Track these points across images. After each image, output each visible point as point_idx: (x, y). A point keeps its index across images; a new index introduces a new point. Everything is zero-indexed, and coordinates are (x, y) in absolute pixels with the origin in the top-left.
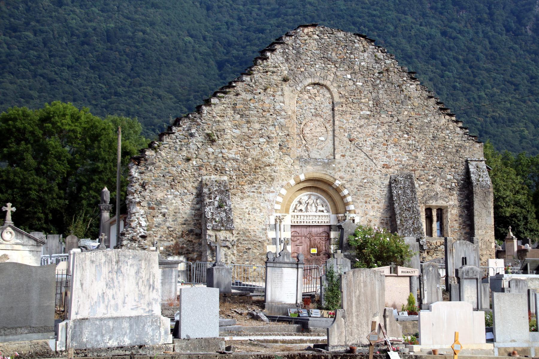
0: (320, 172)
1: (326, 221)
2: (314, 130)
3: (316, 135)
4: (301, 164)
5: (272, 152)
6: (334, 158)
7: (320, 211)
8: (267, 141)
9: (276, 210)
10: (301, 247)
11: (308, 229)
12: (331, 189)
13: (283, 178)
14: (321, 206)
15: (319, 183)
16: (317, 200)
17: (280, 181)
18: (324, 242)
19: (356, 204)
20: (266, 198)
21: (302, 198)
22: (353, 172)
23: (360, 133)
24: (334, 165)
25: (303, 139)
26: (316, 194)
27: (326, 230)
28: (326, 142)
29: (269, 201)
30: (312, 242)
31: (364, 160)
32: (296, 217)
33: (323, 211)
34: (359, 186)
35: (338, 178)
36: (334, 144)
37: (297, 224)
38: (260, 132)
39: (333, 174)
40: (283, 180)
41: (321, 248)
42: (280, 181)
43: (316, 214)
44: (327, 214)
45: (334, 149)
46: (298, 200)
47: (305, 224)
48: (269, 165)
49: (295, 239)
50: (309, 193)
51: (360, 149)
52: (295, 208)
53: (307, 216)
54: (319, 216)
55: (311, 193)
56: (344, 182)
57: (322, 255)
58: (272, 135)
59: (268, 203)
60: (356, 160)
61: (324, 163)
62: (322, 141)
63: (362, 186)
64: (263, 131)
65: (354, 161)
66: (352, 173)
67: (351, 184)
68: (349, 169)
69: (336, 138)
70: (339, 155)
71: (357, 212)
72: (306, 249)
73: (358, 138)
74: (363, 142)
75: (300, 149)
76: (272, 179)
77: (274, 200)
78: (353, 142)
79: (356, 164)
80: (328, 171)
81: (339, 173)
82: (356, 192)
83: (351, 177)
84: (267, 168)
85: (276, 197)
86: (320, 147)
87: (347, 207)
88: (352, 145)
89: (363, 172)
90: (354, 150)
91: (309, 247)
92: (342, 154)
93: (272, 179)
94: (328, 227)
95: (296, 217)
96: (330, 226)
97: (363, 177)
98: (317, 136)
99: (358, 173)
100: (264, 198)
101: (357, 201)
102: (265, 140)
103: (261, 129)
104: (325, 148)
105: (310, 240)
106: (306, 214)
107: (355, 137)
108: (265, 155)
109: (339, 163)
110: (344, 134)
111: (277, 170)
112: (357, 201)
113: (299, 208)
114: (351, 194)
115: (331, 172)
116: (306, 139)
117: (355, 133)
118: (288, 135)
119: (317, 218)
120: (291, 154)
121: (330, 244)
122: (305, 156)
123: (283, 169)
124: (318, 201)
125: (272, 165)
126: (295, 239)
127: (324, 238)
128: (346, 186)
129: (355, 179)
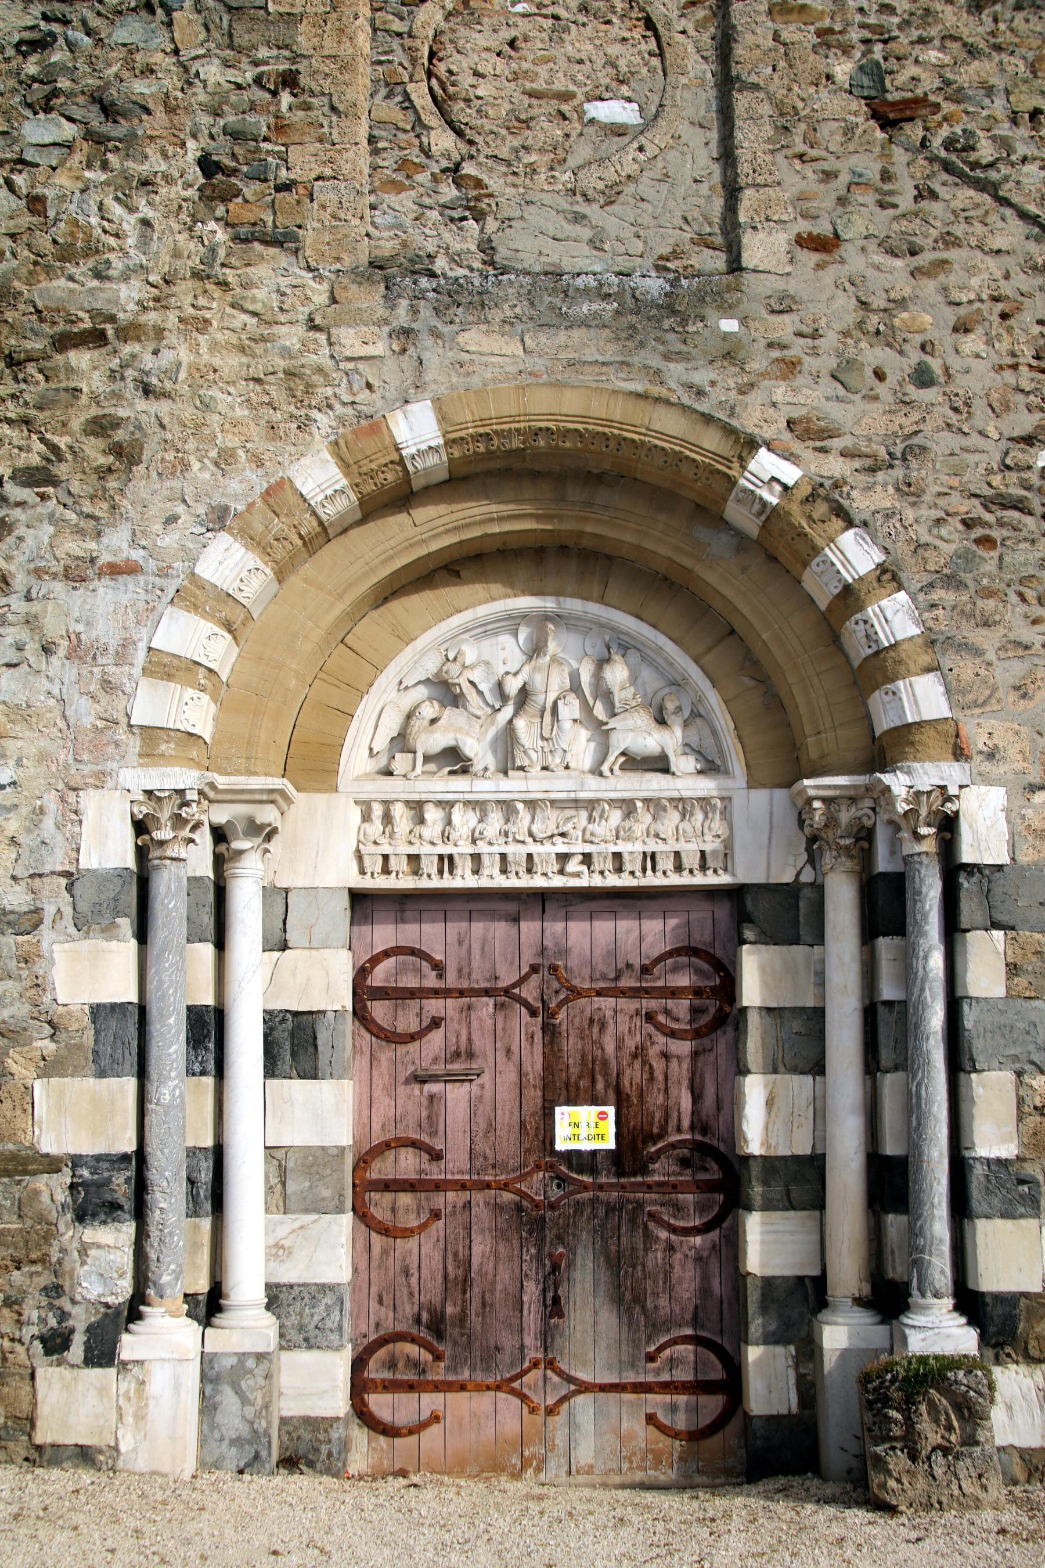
0: (588, 376)
1: (690, 851)
2: (536, 47)
3: (560, 84)
4: (402, 315)
5: (129, 224)
6: (735, 266)
7: (634, 763)
8: (89, 135)
9: (150, 734)
10: (457, 1095)
11: (530, 928)
12: (720, 544)
13: (232, 441)
14: (642, 719)
15: (603, 496)
16: (602, 663)
17: (201, 473)
18: (683, 1047)
19: (966, 668)
20: (53, 627)
21: (470, 654)
22: (923, 378)
23: (972, 51)
24: (729, 325)
25: (431, 118)
26: (595, 609)
27: (701, 937)
28: (657, 139)
29: (78, 651)
30: (571, 1046)
31: (1022, 281)
32: (399, 811)
33: (660, 764)
34: (988, 503)
35: (775, 430)
36: (727, 156)
37: (407, 883)
38: (31, 68)
39: (717, 395)
40: (225, 460)
41: (655, 1100)
42: (201, 473)
43: (593, 788)
44: (706, 786)
45: (732, 191)
46: (430, 666)
47: (492, 878)
48: (96, 338)
49: (408, 1020)
50: (526, 602)
51: (981, 185)
52: (402, 742)
53: (508, 807)
54: (628, 807)
55: (548, 604)
56: (835, 467)
57: (662, 1171)
58: (140, 87)
59: (71, 672)
60: (952, 280)
61: (639, 304)
62: (618, 131)
63: (1019, 506)
64: (58, 56)
65: (929, 287)
66: (914, 392)
67: (908, 490)
68: (874, 355)
69: (742, 102)
70: (782, 239)
71: (977, 738)
72: (507, 1115)
73: (958, 97)
74: (1004, 129)
75: (405, 202)
76: (117, 450)
77: (126, 645)
78: (914, 132)
79: (951, 315)
80: (675, 370)
81: (780, 392)
82: (967, 558)
83: (908, 423)
84: (80, 358)
85: (150, 615)
86: (592, 180)
87: (877, 700)
88: (900, 156)
89: (1025, 378)
90: (925, 193)
91: (534, 1097)
92: (804, 227)
93: (117, 450)
94: (723, 911)
95: (399, 811)
96: (735, 894)
97: (1025, 422)
98: (566, 96)
99: (962, 384)
100: (30, 621)
101: (979, 637)
102: (69, 131)
103: (40, 44)
104: (645, 187)
105: (550, 1030)
106: (486, 787)
107: (929, 83)
108: (66, 254)
109: (783, 304)
110: (819, 63)
111: (172, 372)
112: (979, 637)
113: (436, 741)
114: (914, 578)
115: (701, 377)
116: (459, 111)
117: (933, 55)
118: (289, 80)
119: (600, 829)
120: (308, 237)
121: (743, 1071)
122: (455, 259)
123: (231, 363)
124: (617, 674)
125: (130, 332)
126: (408, 1020)
127: (682, 1007)
128: (860, 504)
129: (944, 443)
